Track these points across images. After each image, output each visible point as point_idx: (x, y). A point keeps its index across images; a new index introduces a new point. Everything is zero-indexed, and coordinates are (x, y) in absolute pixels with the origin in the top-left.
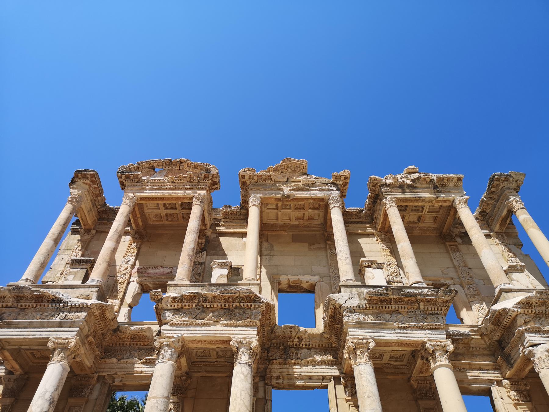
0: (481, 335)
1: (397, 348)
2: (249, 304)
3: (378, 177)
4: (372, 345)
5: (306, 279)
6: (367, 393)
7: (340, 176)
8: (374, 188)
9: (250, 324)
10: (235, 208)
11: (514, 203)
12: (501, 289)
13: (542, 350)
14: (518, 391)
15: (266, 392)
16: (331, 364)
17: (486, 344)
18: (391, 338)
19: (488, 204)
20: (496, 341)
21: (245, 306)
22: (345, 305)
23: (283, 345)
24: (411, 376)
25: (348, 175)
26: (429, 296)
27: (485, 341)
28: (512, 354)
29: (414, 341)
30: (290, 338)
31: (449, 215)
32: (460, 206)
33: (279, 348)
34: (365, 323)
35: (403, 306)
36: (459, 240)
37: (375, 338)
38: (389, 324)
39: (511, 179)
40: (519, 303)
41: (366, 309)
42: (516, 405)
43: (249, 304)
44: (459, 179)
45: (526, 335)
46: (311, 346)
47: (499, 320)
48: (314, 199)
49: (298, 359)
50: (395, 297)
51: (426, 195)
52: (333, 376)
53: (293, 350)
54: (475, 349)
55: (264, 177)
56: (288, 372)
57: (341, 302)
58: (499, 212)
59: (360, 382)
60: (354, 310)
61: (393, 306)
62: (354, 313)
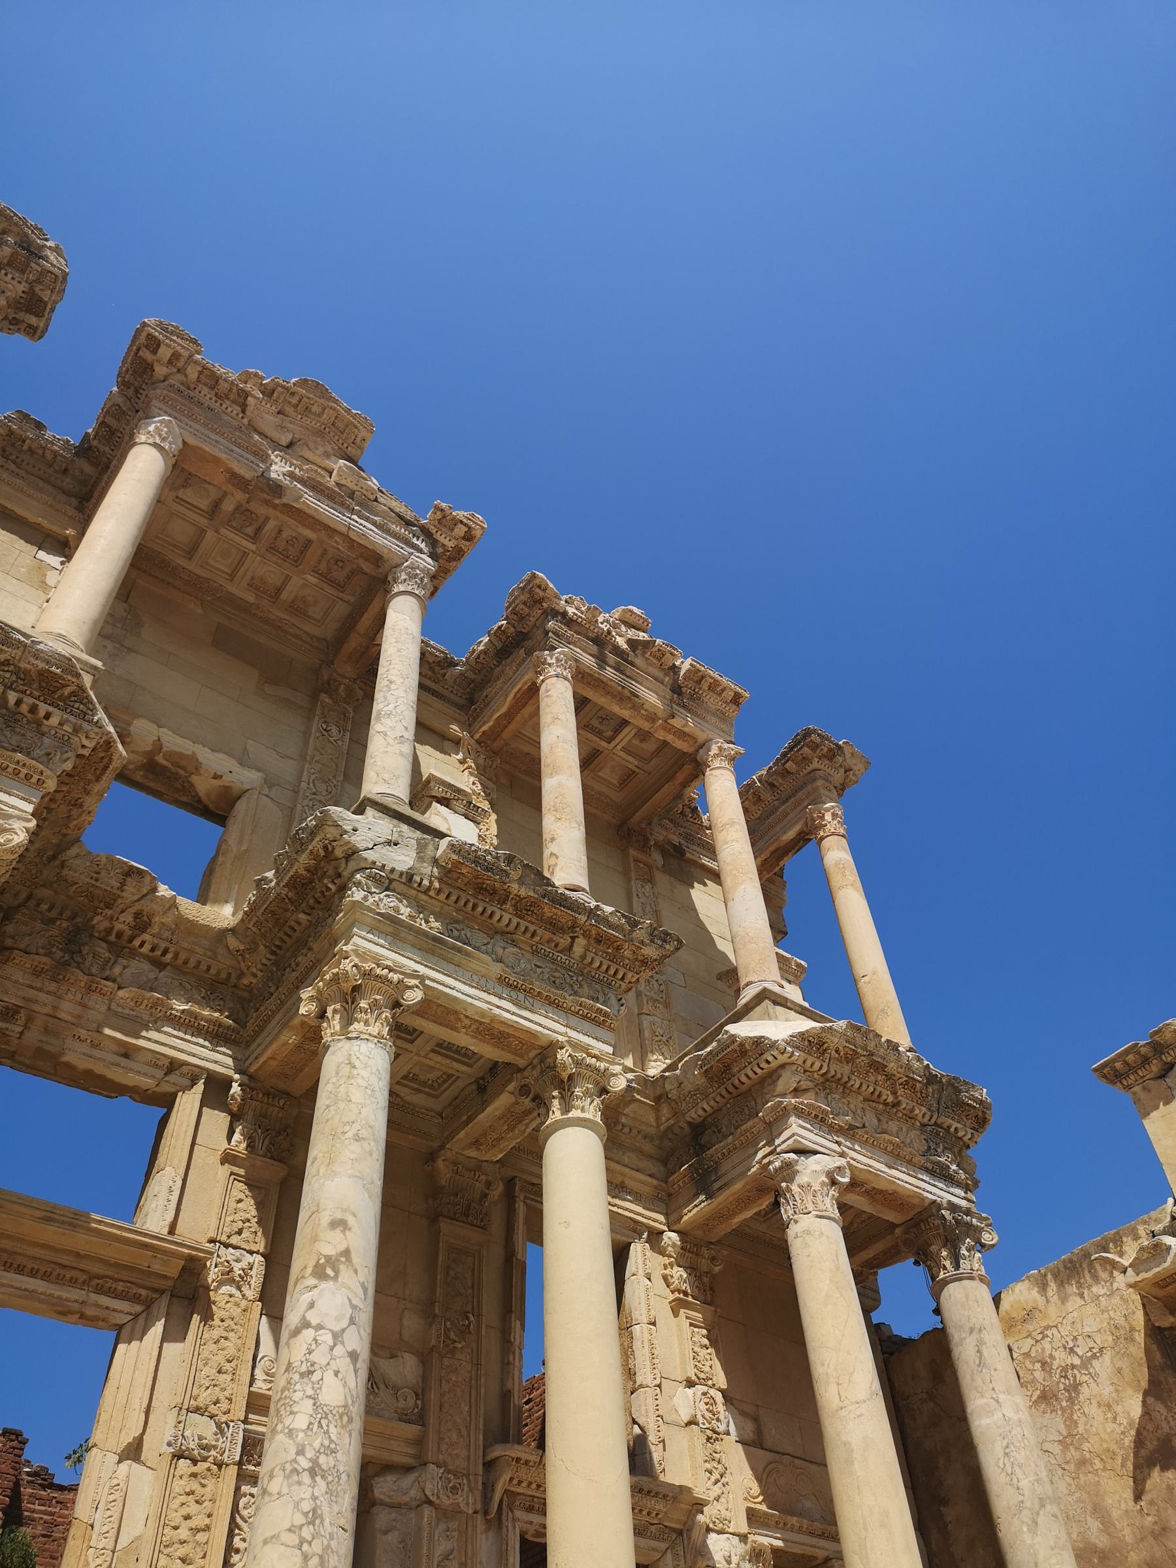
0: (658, 1099)
1: (462, 1039)
2: (43, 708)
3: (551, 586)
4: (414, 996)
5: (217, 766)
6: (356, 1127)
7: (457, 522)
8: (526, 610)
9: (16, 773)
11: (828, 817)
12: (765, 990)
13: (818, 1168)
14: (691, 1269)
16: (216, 1036)
17: (658, 1127)
18: (469, 1000)
19: (759, 799)
20: (689, 1123)
21: (24, 708)
22: (370, 855)
23: (72, 918)
24: (442, 1147)
25: (478, 533)
26: (611, 926)
27: (658, 1118)
28: (725, 1166)
29: (528, 1032)
30: (109, 906)
31: (673, 776)
32: (716, 763)
33: (52, 921)
34: (410, 928)
35: (532, 928)
36: (657, 858)
37: (427, 982)
38: (478, 959)
39: (840, 759)
40: (802, 1034)
41: (426, 892)
42: (677, 1307)
43: (43, 708)
44: (736, 699)
45: (793, 1119)
46: (169, 956)
47: (728, 1068)
48: (352, 543)
49: (106, 979)
50: (523, 893)
51: (651, 698)
52: (207, 1070)
53: (102, 950)
54: (627, 1130)
55: (223, 386)
56: (55, 1008)
57: (359, 840)
58: (777, 829)
59: (342, 1089)
60: (391, 881)
61: (506, 917)
62: (387, 889)
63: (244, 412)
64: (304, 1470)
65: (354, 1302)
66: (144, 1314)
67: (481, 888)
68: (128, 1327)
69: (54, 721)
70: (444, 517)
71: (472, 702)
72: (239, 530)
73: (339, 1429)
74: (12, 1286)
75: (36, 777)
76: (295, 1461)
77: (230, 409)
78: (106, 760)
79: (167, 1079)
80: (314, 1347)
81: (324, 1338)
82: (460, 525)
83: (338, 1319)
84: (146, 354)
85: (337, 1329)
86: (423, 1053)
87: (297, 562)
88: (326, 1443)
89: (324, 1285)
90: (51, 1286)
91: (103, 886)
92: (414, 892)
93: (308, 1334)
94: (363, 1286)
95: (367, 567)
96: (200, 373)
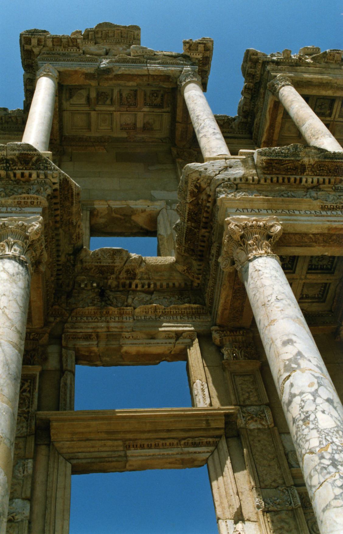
2: (27, 172)
10: (15, 105)
15: (64, 359)
22: (220, 177)
30: (112, 273)
43: (27, 172)
46: (152, 286)
49: (127, 306)
50: (312, 162)
56: (108, 328)
60: (237, 185)
62: (237, 189)
63: (79, 48)
64: (328, 465)
65: (317, 375)
66: (216, 451)
67: (288, 169)
68: (210, 459)
69: (34, 176)
70: (190, 46)
71: (251, 133)
72: (104, 104)
73: (340, 439)
74: (142, 456)
75: (36, 201)
76: (320, 463)
77: (72, 50)
78: (70, 191)
79: (178, 342)
80: (303, 404)
81: (307, 398)
82: (200, 45)
83: (311, 385)
84: (28, 47)
85: (313, 389)
86: (303, 277)
87: (135, 105)
88: (335, 447)
89: (293, 374)
90: (161, 450)
91: (105, 264)
92: (252, 186)
93: (297, 400)
94: (317, 366)
95: (166, 85)
96: (53, 41)
